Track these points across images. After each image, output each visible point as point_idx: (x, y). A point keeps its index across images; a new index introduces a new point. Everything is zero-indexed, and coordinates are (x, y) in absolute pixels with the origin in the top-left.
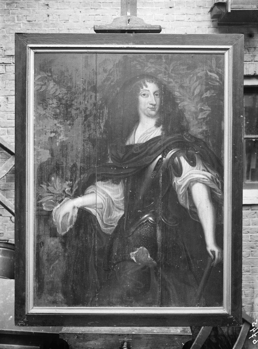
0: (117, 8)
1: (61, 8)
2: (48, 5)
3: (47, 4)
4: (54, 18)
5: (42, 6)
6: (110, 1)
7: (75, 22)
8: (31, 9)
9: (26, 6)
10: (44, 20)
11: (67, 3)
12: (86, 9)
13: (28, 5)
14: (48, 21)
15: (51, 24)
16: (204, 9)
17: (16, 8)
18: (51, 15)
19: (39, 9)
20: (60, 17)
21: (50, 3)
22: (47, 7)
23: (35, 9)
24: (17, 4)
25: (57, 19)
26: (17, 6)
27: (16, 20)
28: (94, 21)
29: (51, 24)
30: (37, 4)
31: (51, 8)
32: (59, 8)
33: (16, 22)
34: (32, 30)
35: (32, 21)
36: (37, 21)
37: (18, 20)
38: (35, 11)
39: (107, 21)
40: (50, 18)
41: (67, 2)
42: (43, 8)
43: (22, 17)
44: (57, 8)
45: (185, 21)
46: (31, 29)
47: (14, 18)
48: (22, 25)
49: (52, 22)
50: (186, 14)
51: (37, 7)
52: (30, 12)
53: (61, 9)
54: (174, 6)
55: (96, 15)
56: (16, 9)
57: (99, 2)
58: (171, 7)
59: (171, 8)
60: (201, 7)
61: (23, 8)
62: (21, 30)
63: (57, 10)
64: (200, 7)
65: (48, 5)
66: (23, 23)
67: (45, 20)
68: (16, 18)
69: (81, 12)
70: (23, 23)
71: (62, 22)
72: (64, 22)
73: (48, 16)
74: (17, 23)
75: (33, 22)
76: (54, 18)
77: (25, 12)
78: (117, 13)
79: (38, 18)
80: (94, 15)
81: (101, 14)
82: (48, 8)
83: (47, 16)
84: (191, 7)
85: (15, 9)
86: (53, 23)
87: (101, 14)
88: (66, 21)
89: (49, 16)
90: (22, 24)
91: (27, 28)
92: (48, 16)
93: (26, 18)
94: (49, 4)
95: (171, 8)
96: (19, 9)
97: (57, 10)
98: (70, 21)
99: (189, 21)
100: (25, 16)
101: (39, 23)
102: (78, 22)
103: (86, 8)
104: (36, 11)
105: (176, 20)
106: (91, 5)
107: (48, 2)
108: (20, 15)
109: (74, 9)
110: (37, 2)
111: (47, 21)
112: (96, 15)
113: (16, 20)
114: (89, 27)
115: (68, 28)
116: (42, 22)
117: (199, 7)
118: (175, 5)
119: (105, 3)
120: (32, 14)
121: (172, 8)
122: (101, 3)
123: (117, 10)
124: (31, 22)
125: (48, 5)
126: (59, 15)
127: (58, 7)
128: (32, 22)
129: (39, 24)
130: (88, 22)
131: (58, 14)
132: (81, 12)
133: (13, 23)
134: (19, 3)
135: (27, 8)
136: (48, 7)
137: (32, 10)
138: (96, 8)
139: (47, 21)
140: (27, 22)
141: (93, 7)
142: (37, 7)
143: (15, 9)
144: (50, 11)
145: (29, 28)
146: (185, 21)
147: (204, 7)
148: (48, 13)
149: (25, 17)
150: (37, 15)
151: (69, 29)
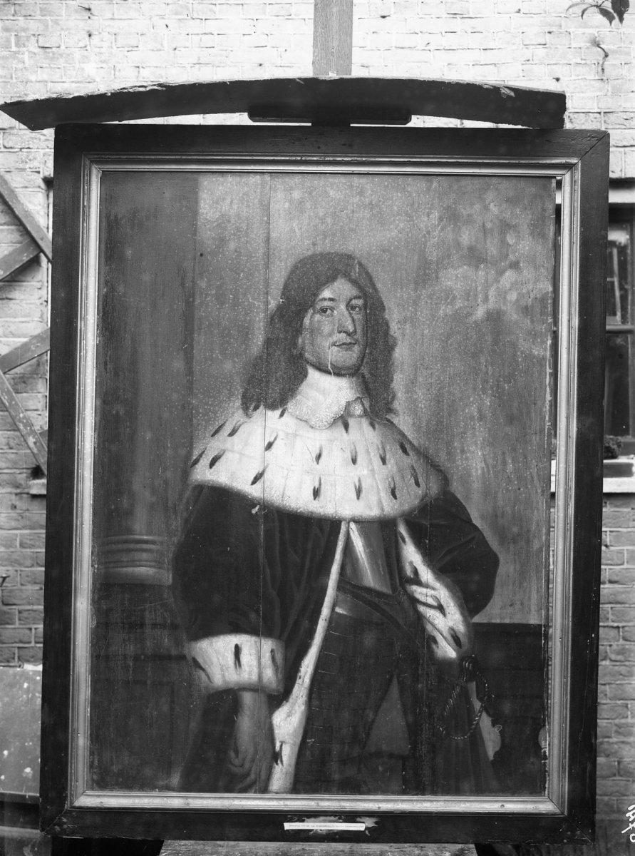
2: (89, 10)
3: (87, 7)
7: (153, 50)
8: (48, 18)
9: (38, 12)
11: (134, 5)
12: (179, 19)
13: (41, 10)
14: (88, 48)
16: (463, 20)
17: (14, 16)
18: (97, 33)
19: (67, 20)
20: (119, 38)
22: (87, 14)
23: (57, 18)
24: (17, 8)
25: (112, 43)
26: (15, 11)
27: (13, 44)
28: (200, 49)
32: (116, 17)
33: (14, 49)
34: (51, 68)
35: (50, 48)
37: (17, 45)
38: (59, 25)
39: (231, 49)
40: (95, 39)
42: (78, 18)
43: (28, 38)
44: (111, 16)
45: (418, 50)
46: (48, 65)
47: (8, 41)
48: (26, 57)
49: (98, 50)
50: (420, 34)
51: (64, 15)
52: (47, 26)
53: (121, 19)
54: (392, 13)
56: (15, 18)
59: (384, 17)
60: (457, 16)
61: (29, 18)
62: (25, 68)
63: (111, 23)
64: (455, 16)
66: (30, 52)
67: (81, 44)
68: (13, 40)
69: (167, 26)
70: (30, 52)
71: (121, 49)
72: (127, 49)
73: (90, 35)
74: (15, 53)
75: (54, 49)
77: (33, 26)
78: (254, 29)
80: (198, 34)
81: (215, 33)
82: (89, 18)
84: (432, 16)
85: (12, 18)
87: (215, 33)
89: (92, 37)
90: (27, 53)
91: (39, 65)
92: (90, 35)
93: (37, 40)
94: (92, 7)
95: (384, 17)
96: (20, 18)
97: (110, 21)
98: (140, 48)
99: (428, 48)
100: (34, 35)
101: (67, 51)
103: (180, 17)
104: (60, 23)
105: (396, 47)
107: (88, 2)
108: (23, 34)
109: (150, 19)
111: (86, 47)
113: (13, 44)
115: (137, 65)
116: (73, 49)
117: (452, 16)
118: (393, 10)
119: (225, 6)
120: (50, 30)
123: (255, 22)
124: (47, 50)
125: (89, 10)
128: (50, 50)
130: (183, 50)
131: (114, 32)
132: (167, 26)
133: (8, 53)
134: (20, 5)
135: (40, 17)
136: (90, 15)
137: (51, 20)
138: (204, 18)
139: (86, 47)
140: (38, 50)
141: (198, 14)
142: (64, 15)
143: (12, 18)
144: (95, 24)
145: (44, 65)
146: (418, 50)
147: (464, 16)
148: (87, 28)
149: (33, 39)
150: (63, 33)
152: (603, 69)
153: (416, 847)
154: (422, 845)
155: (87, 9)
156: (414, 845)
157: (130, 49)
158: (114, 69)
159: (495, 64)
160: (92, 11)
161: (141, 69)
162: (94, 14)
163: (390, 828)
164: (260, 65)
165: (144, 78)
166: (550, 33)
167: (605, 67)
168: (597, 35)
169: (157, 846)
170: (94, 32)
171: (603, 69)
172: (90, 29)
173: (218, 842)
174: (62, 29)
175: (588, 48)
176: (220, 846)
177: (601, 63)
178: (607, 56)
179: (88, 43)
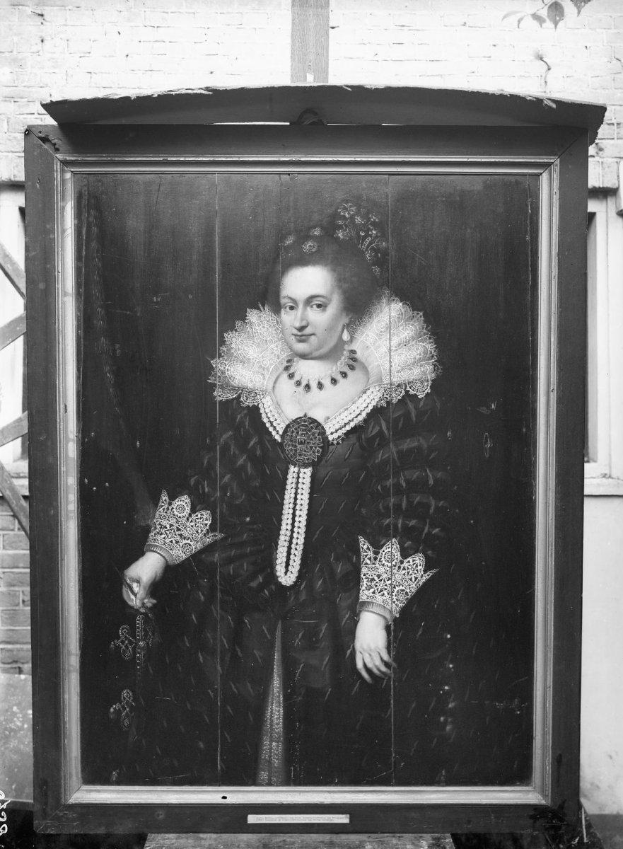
0: (207, 26)
1: (72, 23)
3: (40, 13)
4: (55, 46)
5: (29, 16)
6: (190, 11)
10: (32, 51)
11: (87, 12)
14: (41, 53)
15: (49, 60)
21: (46, 11)
29: (49, 60)
30: (17, 13)
31: (50, 22)
32: (68, 23)
36: (15, 53)
41: (87, 10)
44: (65, 23)
55: (156, 41)
57: (164, 12)
58: (334, 26)
64: (402, 28)
65: (42, 15)
67: (35, 49)
73: (42, 41)
75: (7, 54)
76: (55, 46)
79: (17, 44)
83: (40, 41)
86: (53, 59)
88: (85, 53)
89: (45, 42)
92: (42, 41)
99: (376, 58)
102: (113, 56)
103: (132, 24)
106: (145, 19)
110: (15, 7)
112: (156, 41)
114: (139, 70)
121: (336, 29)
122: (167, 13)
125: (42, 15)
126: (68, 40)
127: (66, 20)
129: (21, 60)
138: (156, 26)
144: (47, 29)
147: (411, 28)
151: (90, 73)
152: (546, 82)
153: (394, 837)
154: (398, 835)
155: (39, 15)
156: (391, 835)
157: (82, 55)
158: (67, 75)
159: (441, 75)
160: (45, 17)
161: (94, 76)
162: (47, 20)
163: (366, 820)
164: (211, 73)
165: (96, 84)
166: (495, 46)
167: (548, 80)
168: (540, 49)
169: (142, 839)
170: (45, 38)
171: (546, 82)
172: (43, 35)
173: (201, 835)
174: (15, 34)
175: (531, 61)
176: (203, 839)
177: (544, 76)
178: (549, 69)
179: (40, 48)
